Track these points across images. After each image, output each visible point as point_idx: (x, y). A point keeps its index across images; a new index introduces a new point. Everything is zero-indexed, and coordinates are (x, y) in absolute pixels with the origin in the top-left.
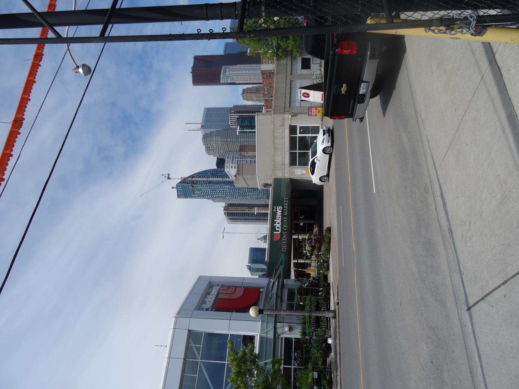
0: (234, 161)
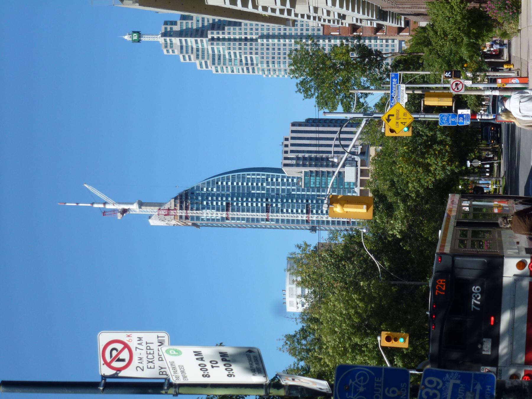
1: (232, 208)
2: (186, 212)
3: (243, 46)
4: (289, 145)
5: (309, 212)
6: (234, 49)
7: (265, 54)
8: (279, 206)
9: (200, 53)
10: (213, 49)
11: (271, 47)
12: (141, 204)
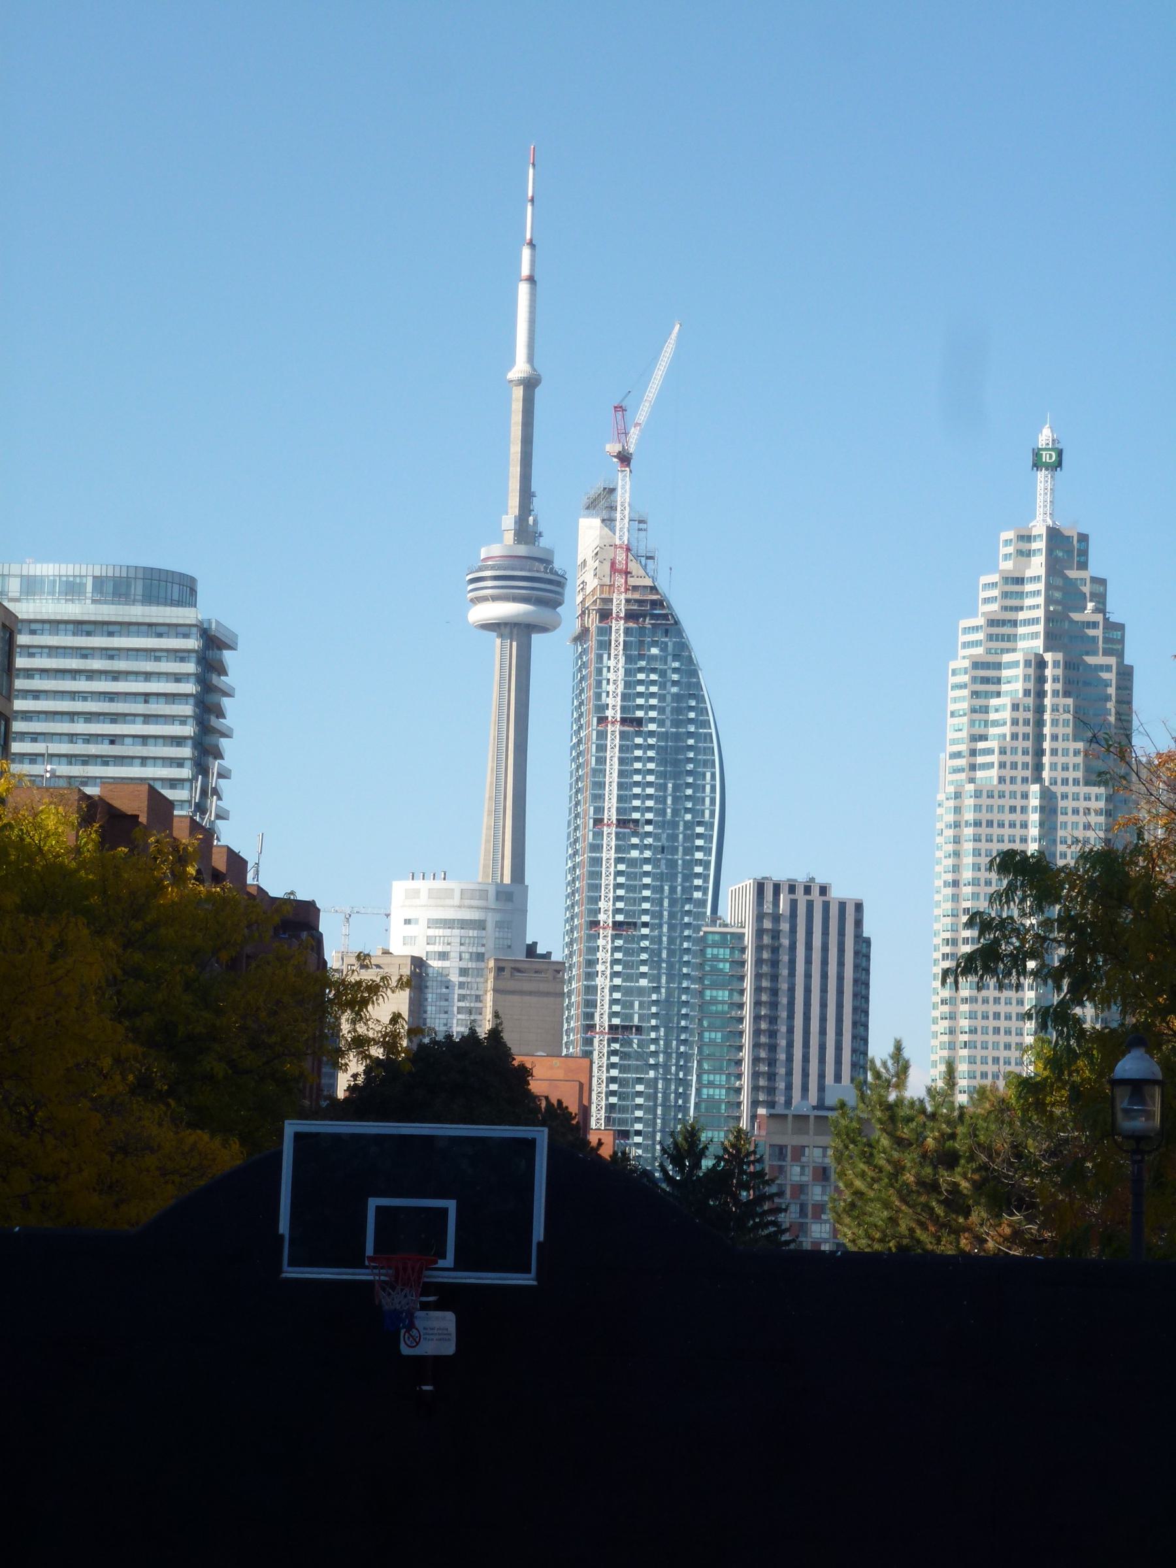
0: (448, 932)
1: (628, 732)
2: (621, 618)
3: (1021, 744)
4: (809, 898)
5: (616, 930)
6: (1015, 722)
7: (1001, 802)
8: (632, 852)
9: (1006, 630)
10: (1015, 664)
11: (1017, 817)
12: (530, 384)
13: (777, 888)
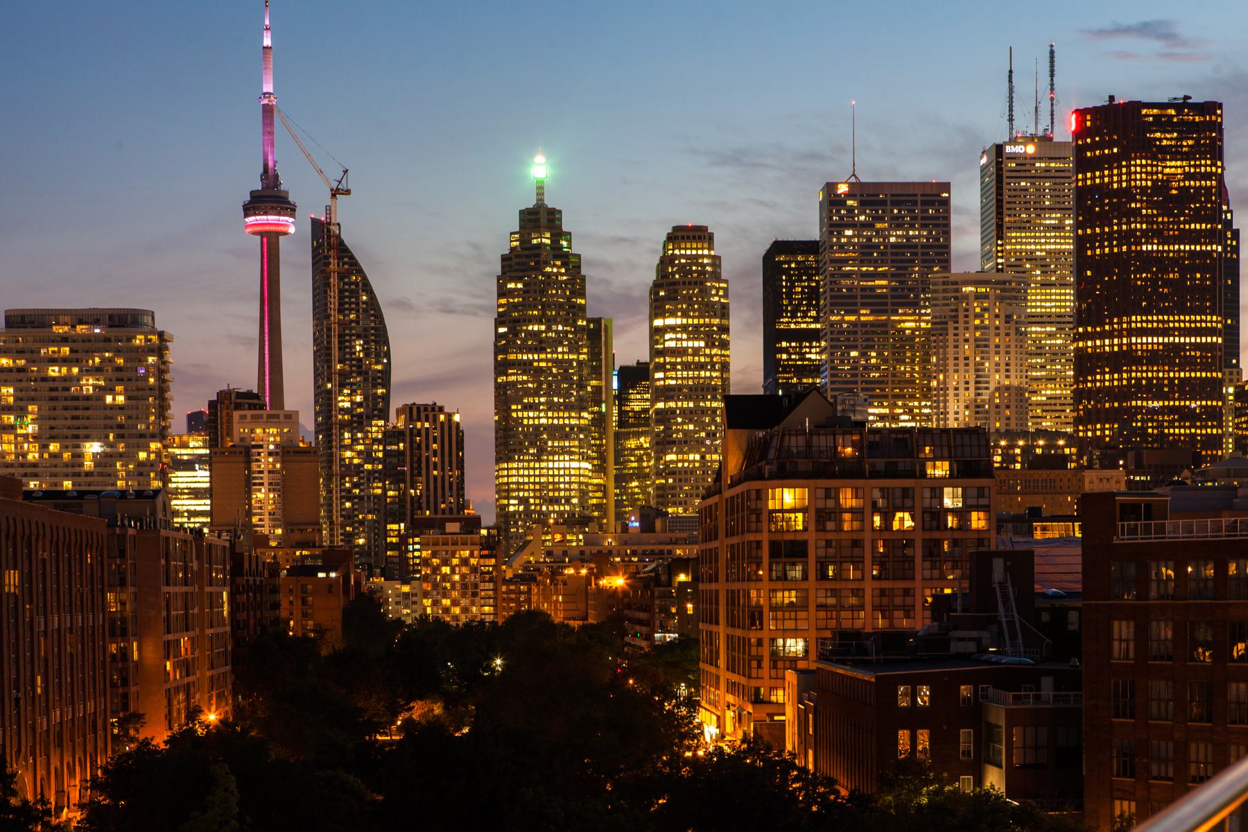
13: (418, 409)
